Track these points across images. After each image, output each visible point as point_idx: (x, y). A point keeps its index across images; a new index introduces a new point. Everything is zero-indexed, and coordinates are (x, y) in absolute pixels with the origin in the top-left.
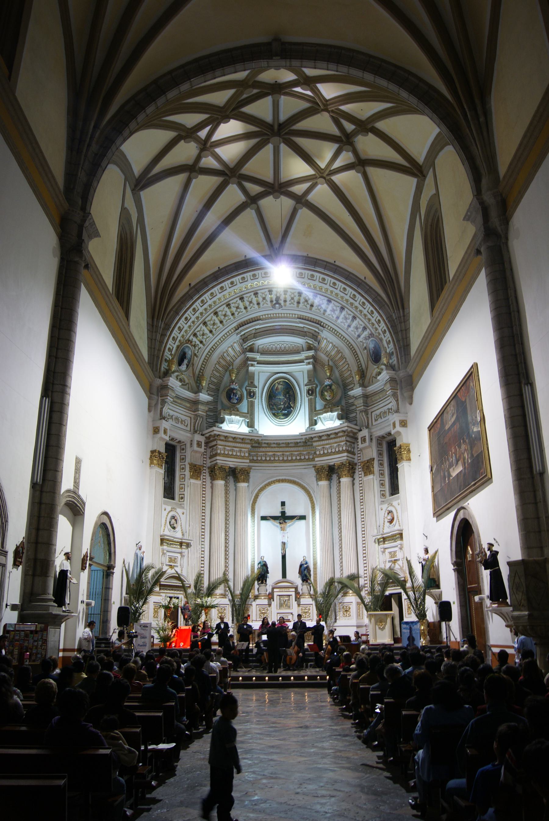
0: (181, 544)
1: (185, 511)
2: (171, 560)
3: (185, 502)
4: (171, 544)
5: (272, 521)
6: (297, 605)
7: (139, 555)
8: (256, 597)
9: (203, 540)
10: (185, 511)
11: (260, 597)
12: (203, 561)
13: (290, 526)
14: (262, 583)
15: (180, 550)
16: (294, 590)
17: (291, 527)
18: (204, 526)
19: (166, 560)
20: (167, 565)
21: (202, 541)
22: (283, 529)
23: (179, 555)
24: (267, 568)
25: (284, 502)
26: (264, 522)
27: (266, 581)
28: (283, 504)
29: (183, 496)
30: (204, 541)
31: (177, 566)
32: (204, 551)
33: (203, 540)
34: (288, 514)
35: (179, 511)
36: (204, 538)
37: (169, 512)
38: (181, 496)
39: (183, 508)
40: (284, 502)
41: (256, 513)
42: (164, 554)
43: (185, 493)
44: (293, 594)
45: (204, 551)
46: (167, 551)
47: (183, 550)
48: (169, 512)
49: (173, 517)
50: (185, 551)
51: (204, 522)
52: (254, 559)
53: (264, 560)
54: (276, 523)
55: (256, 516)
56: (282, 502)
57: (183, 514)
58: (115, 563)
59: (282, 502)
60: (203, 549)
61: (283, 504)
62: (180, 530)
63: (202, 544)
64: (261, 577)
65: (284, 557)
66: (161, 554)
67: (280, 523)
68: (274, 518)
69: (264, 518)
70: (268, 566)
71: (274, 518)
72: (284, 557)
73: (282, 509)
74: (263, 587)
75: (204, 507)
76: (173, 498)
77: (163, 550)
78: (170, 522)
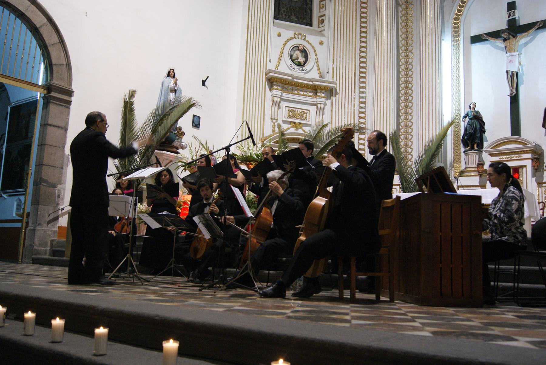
0: (315, 89)
1: (324, 39)
2: (292, 113)
3: (326, 28)
4: (292, 90)
5: (492, 40)
6: (535, 185)
7: (166, 85)
8: (462, 174)
9: (362, 85)
10: (324, 39)
11: (466, 174)
12: (364, 118)
13: (526, 44)
14: (472, 148)
15: (313, 100)
16: (529, 156)
17: (529, 45)
18: (365, 63)
19: (282, 115)
20: (284, 122)
21: (360, 87)
22: (508, 49)
23: (313, 109)
24: (482, 123)
25: (514, 3)
26: (477, 47)
27: (480, 146)
28: (511, 6)
29: (323, 18)
30: (364, 88)
31: (309, 125)
32: (364, 103)
33: (362, 85)
34: (523, 21)
35: (314, 39)
36: (365, 83)
37: (291, 39)
38: (321, 19)
39: (323, 35)
40: (514, 3)
41: (461, 32)
42: (277, 104)
43: (327, 13)
44: (529, 163)
45: (364, 103)
46: (282, 100)
47: (319, 100)
48: (291, 39)
49: (296, 48)
50: (320, 99)
51: (365, 57)
52: (459, 110)
53: (476, 110)
54: (500, 43)
55: (461, 38)
56: (508, 4)
57: (321, 43)
58: (70, 84)
59: (508, 4)
60: (362, 100)
61: (511, 6)
62: (315, 68)
63: (361, 92)
64: (468, 139)
65: (514, 100)
66: (269, 102)
67: (505, 40)
68: (495, 35)
69: (476, 39)
70: (484, 119)
71: (495, 35)
72: (514, 100)
73: (510, 15)
74: (473, 158)
75: (365, 32)
76: (310, 24)
77: (273, 97)
78: (291, 56)
